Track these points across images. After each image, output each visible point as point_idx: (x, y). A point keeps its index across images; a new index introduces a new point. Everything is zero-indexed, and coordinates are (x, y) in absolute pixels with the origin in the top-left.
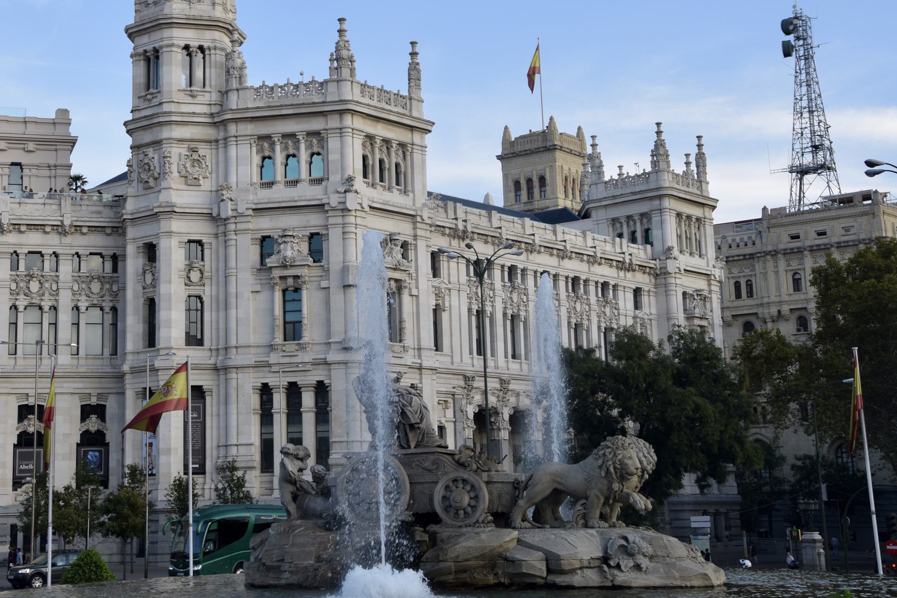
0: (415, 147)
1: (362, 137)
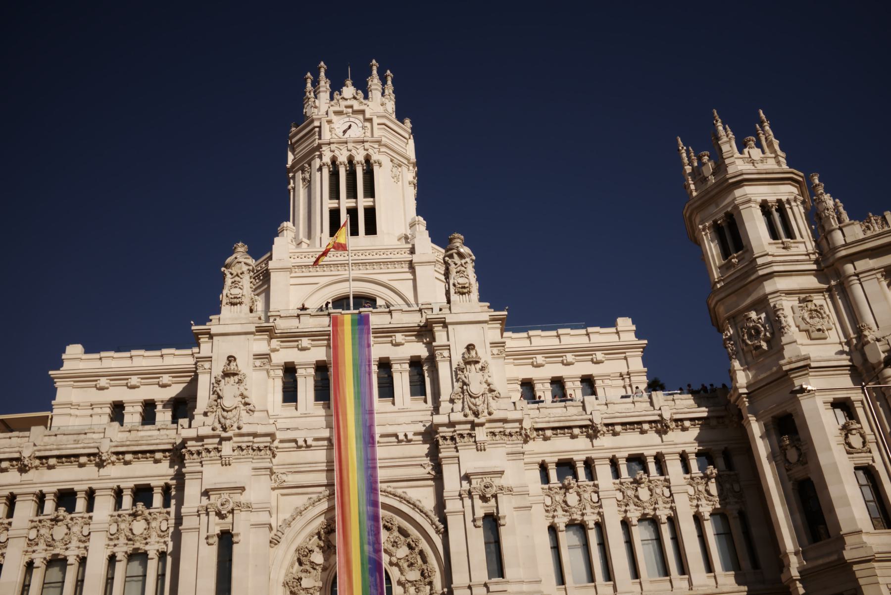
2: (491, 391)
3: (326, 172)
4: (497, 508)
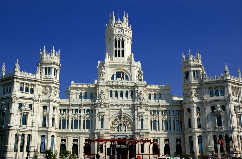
2: (144, 99)
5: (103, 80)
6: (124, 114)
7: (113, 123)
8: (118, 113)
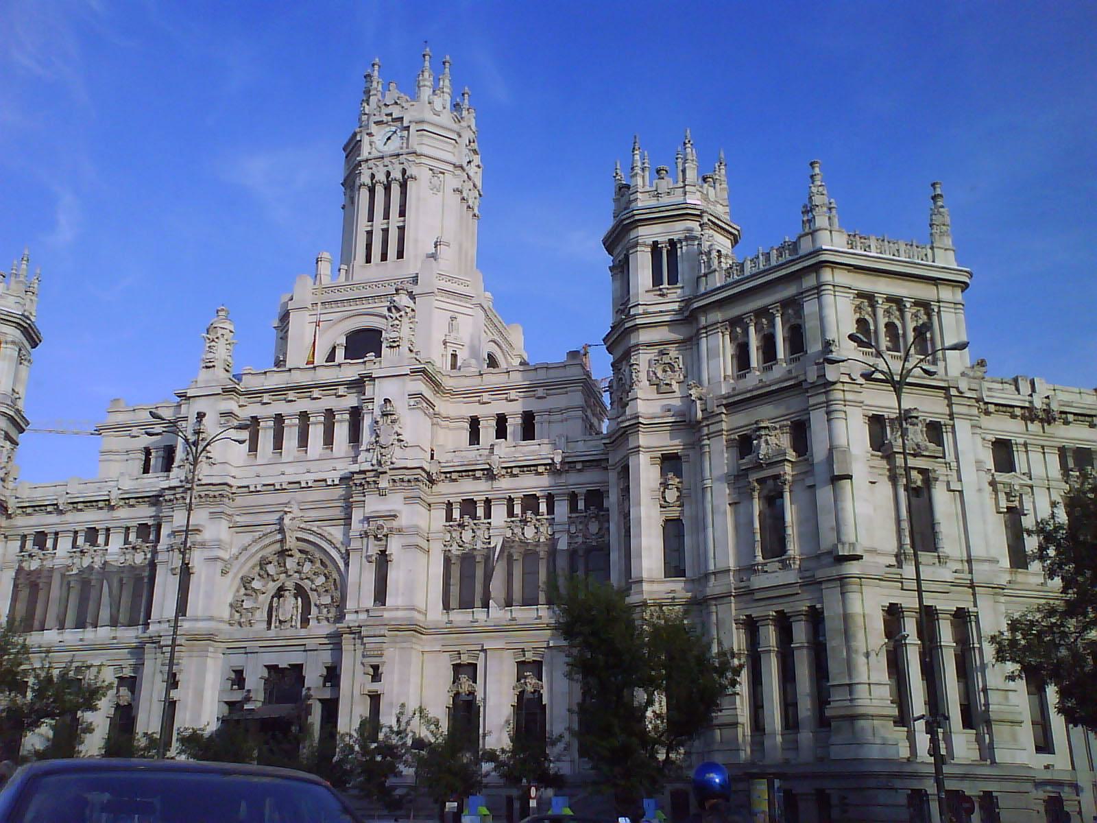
0: (941, 304)
1: (852, 296)
3: (364, 194)
4: (386, 546)
5: (214, 366)
6: (300, 535)
7: (246, 582)
8: (268, 529)
